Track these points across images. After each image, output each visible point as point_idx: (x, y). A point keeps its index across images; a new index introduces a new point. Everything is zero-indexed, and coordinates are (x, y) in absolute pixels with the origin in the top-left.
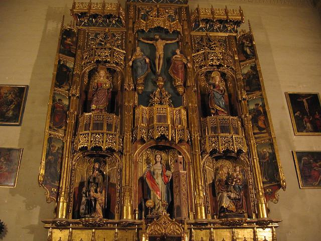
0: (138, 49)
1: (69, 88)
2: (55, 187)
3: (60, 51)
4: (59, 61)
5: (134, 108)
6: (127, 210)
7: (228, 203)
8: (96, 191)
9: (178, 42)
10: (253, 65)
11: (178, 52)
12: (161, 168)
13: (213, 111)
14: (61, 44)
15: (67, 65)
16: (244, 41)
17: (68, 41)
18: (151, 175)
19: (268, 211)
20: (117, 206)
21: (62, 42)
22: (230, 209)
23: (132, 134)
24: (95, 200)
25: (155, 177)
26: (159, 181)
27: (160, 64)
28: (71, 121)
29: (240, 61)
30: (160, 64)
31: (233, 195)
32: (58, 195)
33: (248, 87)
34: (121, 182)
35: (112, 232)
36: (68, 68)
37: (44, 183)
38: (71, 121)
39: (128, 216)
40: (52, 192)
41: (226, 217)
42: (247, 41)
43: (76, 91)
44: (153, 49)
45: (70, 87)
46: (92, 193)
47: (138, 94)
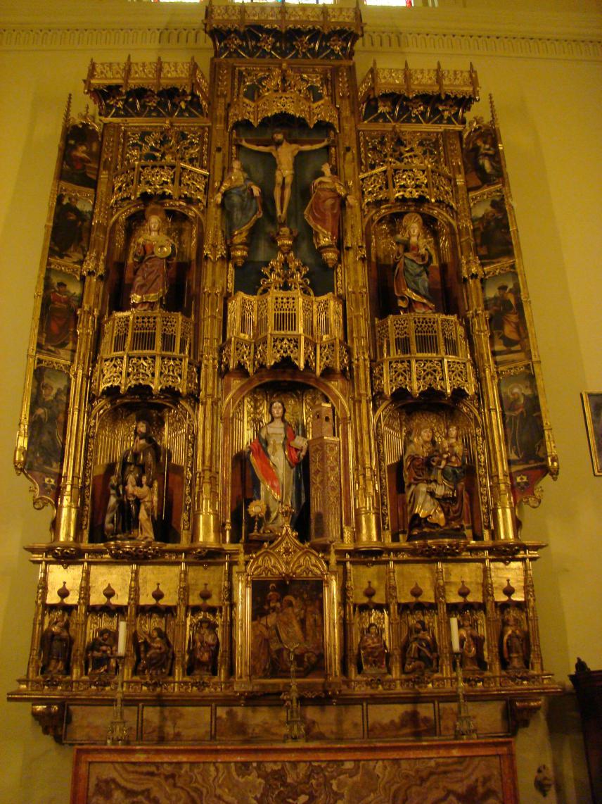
3: (61, 176)
4: (60, 199)
5: (227, 298)
12: (282, 431)
17: (81, 152)
23: (221, 357)
38: (85, 330)
43: (94, 263)
47: (235, 267)
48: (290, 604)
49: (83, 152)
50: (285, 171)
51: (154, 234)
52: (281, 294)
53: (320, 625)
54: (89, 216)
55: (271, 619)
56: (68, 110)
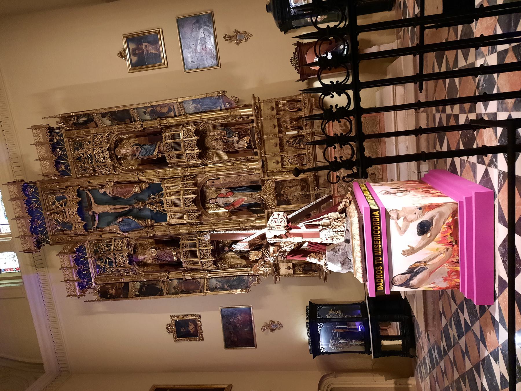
6: (259, 223)
10: (101, 115)
11: (102, 191)
12: (221, 199)
13: (160, 156)
15: (139, 287)
16: (71, 122)
19: (246, 106)
25: (229, 203)
27: (119, 208)
29: (97, 126)
30: (119, 208)
31: (236, 139)
36: (141, 287)
41: (255, 145)
42: (71, 120)
43: (163, 276)
44: (101, 215)
48: (284, 192)
49: (112, 291)
50: (107, 208)
52: (165, 205)
54: (142, 283)
55: (290, 198)
56: (93, 301)
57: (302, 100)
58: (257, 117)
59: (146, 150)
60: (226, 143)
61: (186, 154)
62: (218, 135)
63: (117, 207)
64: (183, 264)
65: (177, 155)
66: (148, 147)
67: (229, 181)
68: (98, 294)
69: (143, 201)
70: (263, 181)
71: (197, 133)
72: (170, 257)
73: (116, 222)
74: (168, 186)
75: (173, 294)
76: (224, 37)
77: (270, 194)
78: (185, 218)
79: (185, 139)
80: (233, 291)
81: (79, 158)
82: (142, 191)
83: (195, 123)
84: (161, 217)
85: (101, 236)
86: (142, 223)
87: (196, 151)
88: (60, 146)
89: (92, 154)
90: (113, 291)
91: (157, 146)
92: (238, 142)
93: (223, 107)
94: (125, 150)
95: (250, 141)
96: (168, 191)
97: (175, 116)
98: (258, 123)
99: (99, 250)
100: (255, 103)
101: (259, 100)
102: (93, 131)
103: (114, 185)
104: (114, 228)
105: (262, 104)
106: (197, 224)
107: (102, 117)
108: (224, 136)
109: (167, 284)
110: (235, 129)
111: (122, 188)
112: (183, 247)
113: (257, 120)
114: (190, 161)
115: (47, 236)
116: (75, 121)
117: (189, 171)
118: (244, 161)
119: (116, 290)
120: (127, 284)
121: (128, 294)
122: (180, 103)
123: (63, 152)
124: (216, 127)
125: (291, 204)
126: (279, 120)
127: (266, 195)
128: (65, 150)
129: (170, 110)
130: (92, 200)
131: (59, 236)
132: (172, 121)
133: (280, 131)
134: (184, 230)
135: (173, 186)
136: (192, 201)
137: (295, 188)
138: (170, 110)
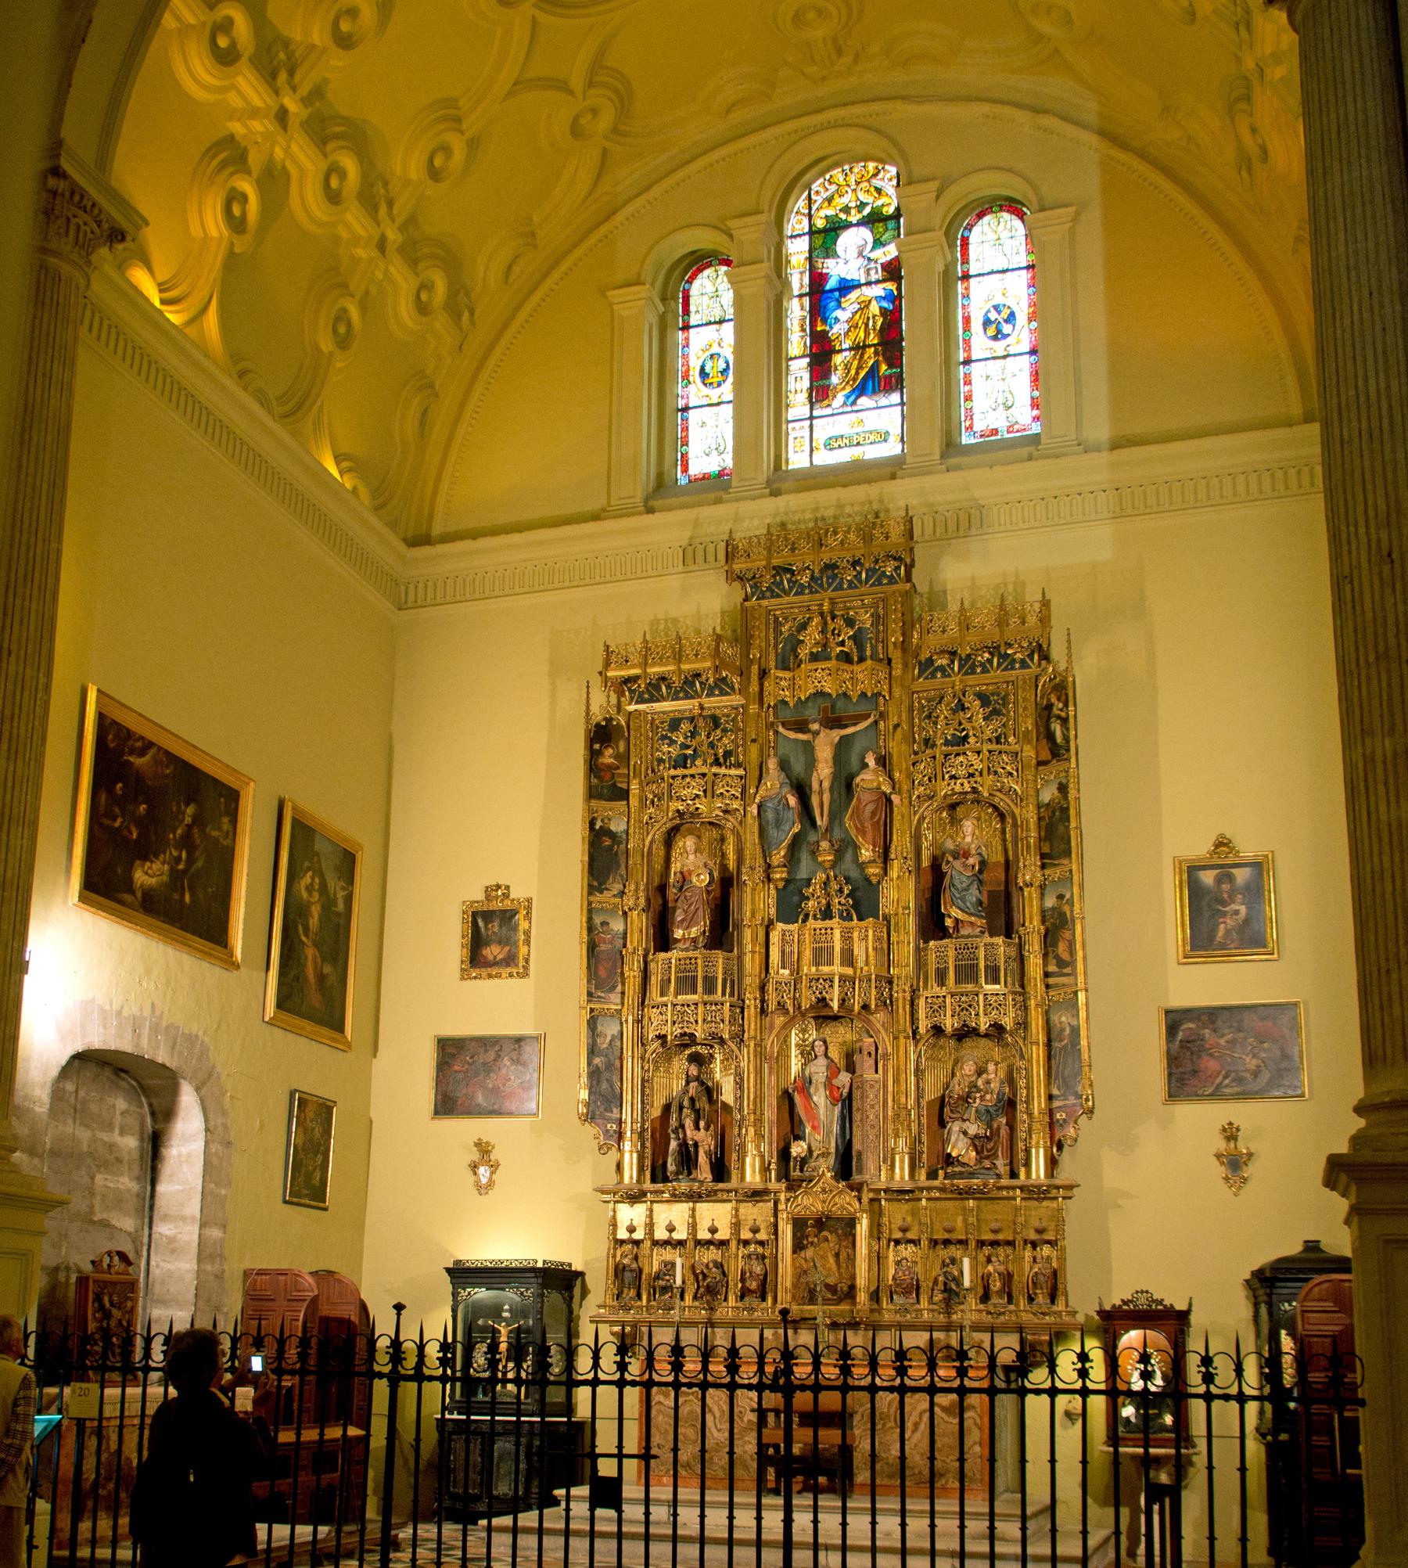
0: (772, 764)
1: (621, 886)
2: (609, 1120)
3: (592, 794)
5: (768, 927)
7: (960, 1144)
8: (697, 1128)
9: (876, 722)
11: (871, 761)
13: (949, 922)
14: (591, 770)
15: (613, 828)
16: (1054, 700)
18: (805, 1084)
19: (1052, 1163)
20: (734, 1156)
21: (593, 767)
22: (965, 1160)
24: (696, 1145)
25: (812, 1090)
26: (820, 1098)
28: (632, 972)
29: (1039, 763)
30: (821, 801)
31: (973, 1129)
32: (620, 1136)
33: (1048, 844)
34: (742, 1105)
35: (729, 1206)
37: (590, 1117)
39: (752, 1176)
40: (607, 1131)
41: (954, 1176)
43: (636, 896)
44: (809, 748)
45: (625, 886)
46: (688, 1132)
48: (827, 1240)
49: (610, 757)
50: (823, 772)
51: (691, 857)
52: (819, 924)
53: (852, 1259)
54: (624, 836)
55: (809, 1253)
57: (1055, 1308)
58: (1022, 1188)
59: (967, 889)
60: (966, 1099)
61: (944, 997)
62: (988, 1082)
63: (826, 797)
64: (662, 955)
65: (946, 969)
66: (971, 894)
67: (867, 1097)
68: (605, 719)
69: (834, 865)
70: (858, 1188)
71: (998, 1029)
72: (683, 920)
73: (786, 789)
74: (867, 936)
75: (590, 920)
76: (1230, 1124)
77: (824, 1202)
78: (782, 971)
79: (981, 997)
80: (584, 1079)
81: (962, 707)
82: (861, 867)
83: (1023, 1025)
84: (790, 907)
85: (754, 741)
86: (778, 856)
87: (949, 1023)
88: (995, 660)
89: (967, 746)
90: (608, 758)
91: (973, 919)
92: (965, 1133)
93: (1056, 1104)
94: (971, 832)
95: (964, 1164)
96: (856, 935)
97: (1047, 975)
98: (1007, 1188)
99: (718, 732)
100: (1058, 1188)
101: (1064, 1198)
102: (1029, 752)
103: (885, 794)
104: (774, 780)
105: (1054, 1204)
106: (763, 1001)
107: (1060, 784)
108: (982, 1098)
109: (616, 906)
110: (999, 1128)
111: (872, 818)
112: (706, 960)
113: (1013, 1188)
114: (926, 1002)
115: (768, 594)
116: (1055, 711)
117: (901, 993)
118: (916, 1141)
119: (610, 767)
120: (624, 795)
121: (599, 799)
122: (1075, 993)
123: (982, 665)
124: (1011, 1080)
125: (794, 1252)
126: (1011, 1243)
127: (824, 1191)
128: (985, 671)
129: (1062, 964)
130: (850, 730)
131: (763, 627)
132: (1035, 965)
133: (981, 1244)
134: (751, 964)
135: (867, 949)
136: (824, 999)
137: (834, 1267)
138: (1062, 964)
